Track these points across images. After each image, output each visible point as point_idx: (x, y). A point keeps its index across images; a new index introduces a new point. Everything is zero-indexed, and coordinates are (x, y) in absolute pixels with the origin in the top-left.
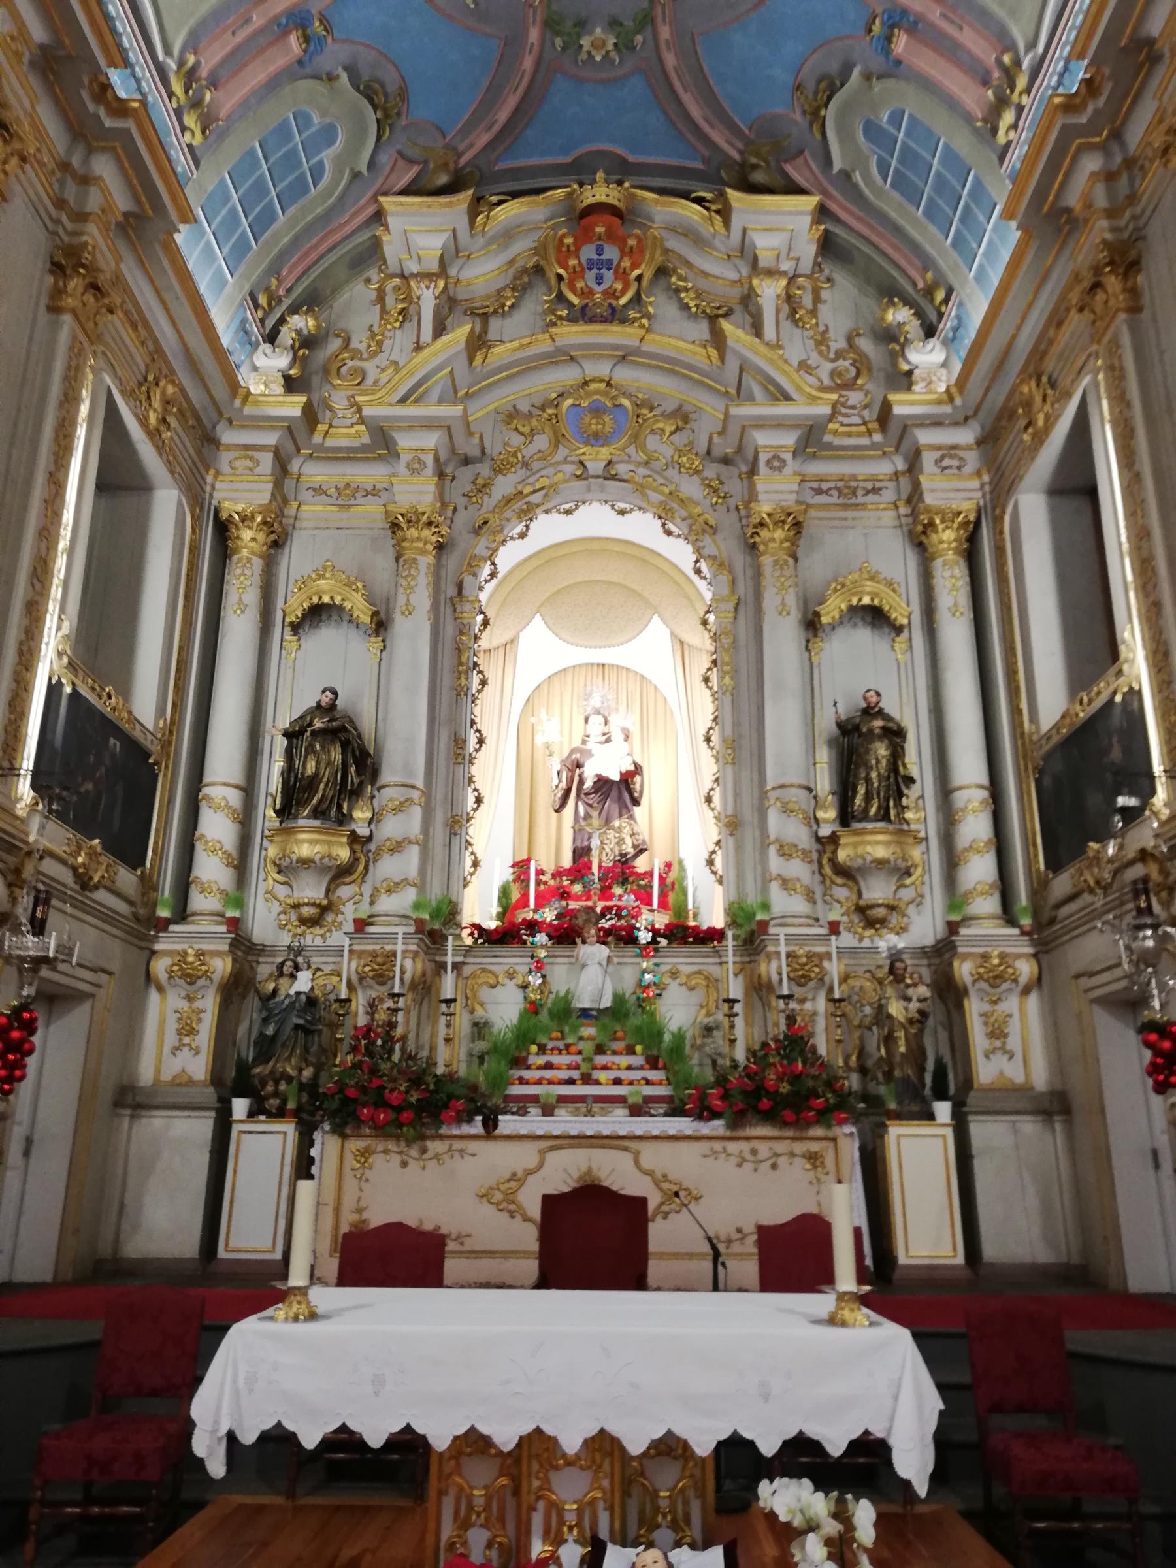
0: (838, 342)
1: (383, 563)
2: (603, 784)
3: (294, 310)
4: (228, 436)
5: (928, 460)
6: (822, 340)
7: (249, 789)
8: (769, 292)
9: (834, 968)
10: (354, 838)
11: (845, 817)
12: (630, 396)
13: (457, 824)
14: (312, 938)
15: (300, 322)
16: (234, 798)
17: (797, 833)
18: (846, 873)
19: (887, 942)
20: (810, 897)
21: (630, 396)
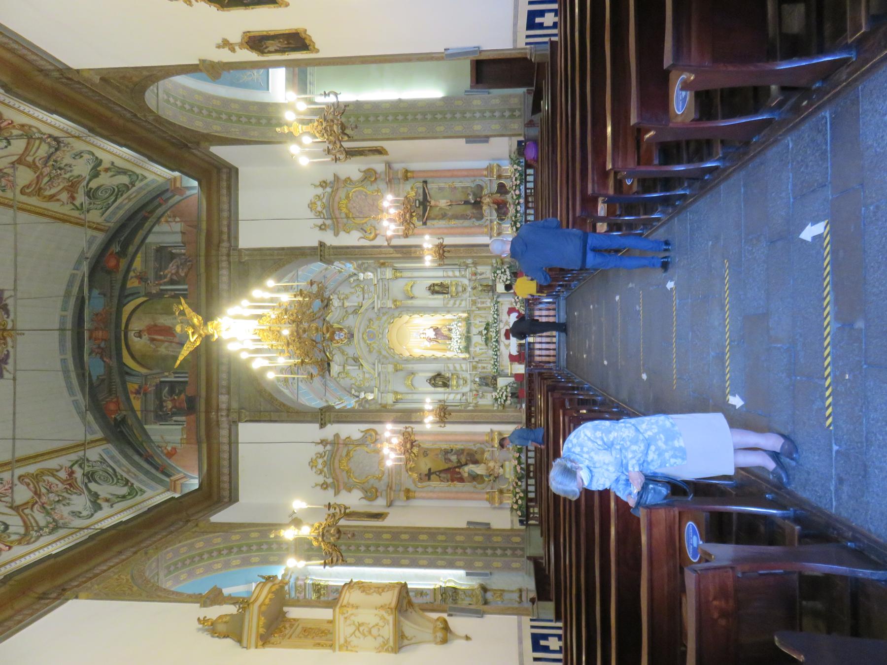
0: (353, 290)
1: (401, 374)
2: (436, 335)
3: (351, 393)
4: (380, 402)
5: (383, 277)
6: (352, 293)
7: (445, 393)
8: (347, 304)
9: (474, 298)
10: (452, 375)
11: (447, 293)
12: (365, 330)
13: (449, 359)
14: (469, 382)
15: (353, 392)
16: (446, 395)
17: (452, 302)
18: (457, 293)
19: (469, 289)
20: (462, 300)
21: (365, 330)
